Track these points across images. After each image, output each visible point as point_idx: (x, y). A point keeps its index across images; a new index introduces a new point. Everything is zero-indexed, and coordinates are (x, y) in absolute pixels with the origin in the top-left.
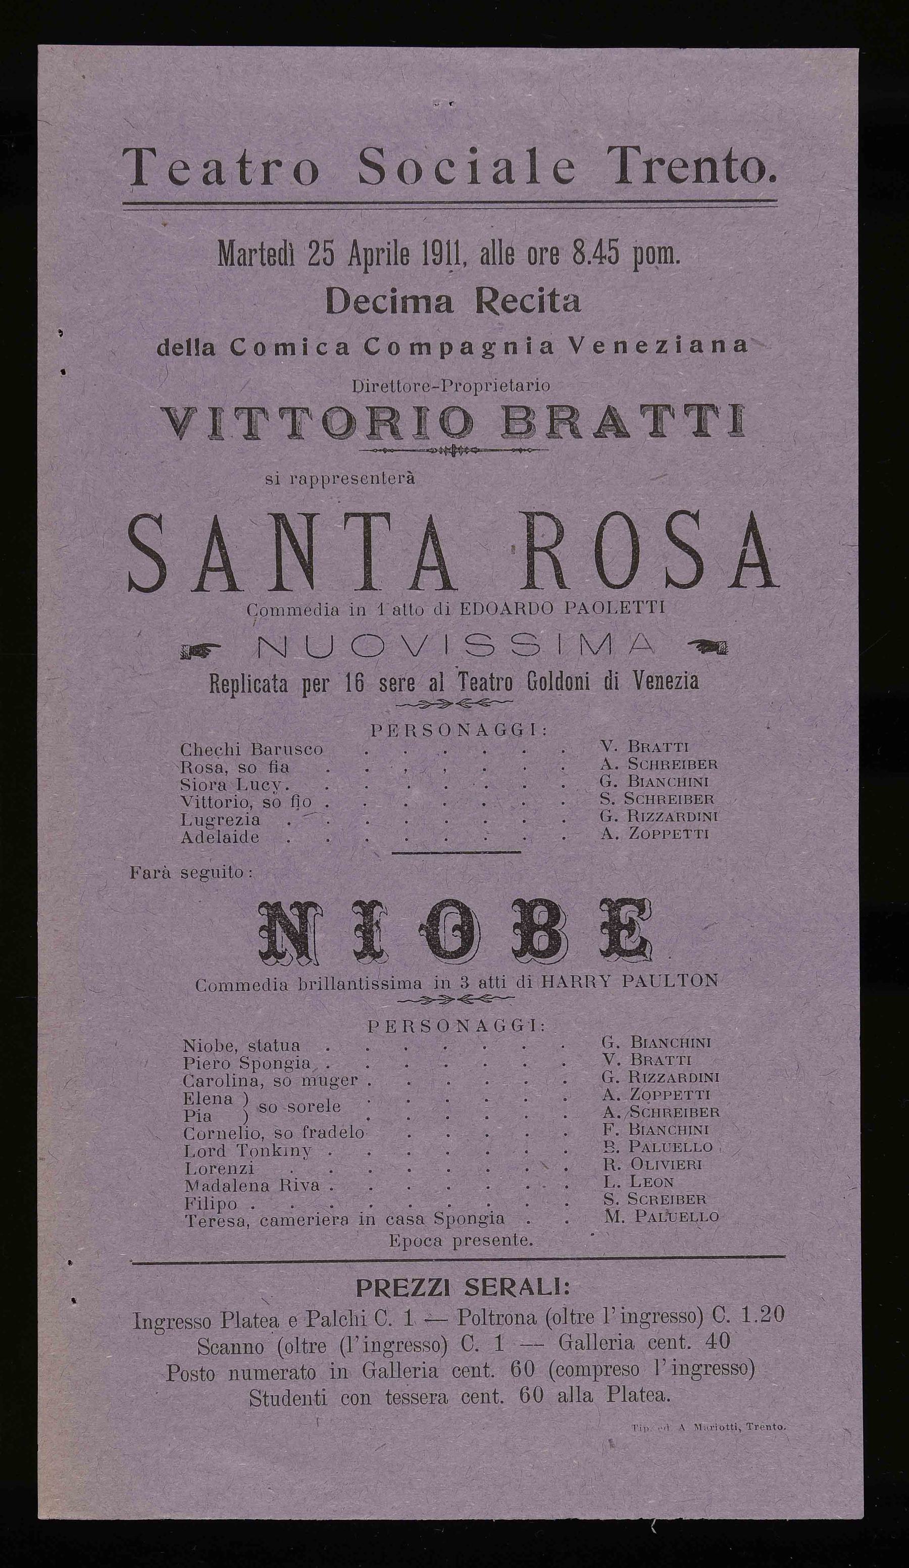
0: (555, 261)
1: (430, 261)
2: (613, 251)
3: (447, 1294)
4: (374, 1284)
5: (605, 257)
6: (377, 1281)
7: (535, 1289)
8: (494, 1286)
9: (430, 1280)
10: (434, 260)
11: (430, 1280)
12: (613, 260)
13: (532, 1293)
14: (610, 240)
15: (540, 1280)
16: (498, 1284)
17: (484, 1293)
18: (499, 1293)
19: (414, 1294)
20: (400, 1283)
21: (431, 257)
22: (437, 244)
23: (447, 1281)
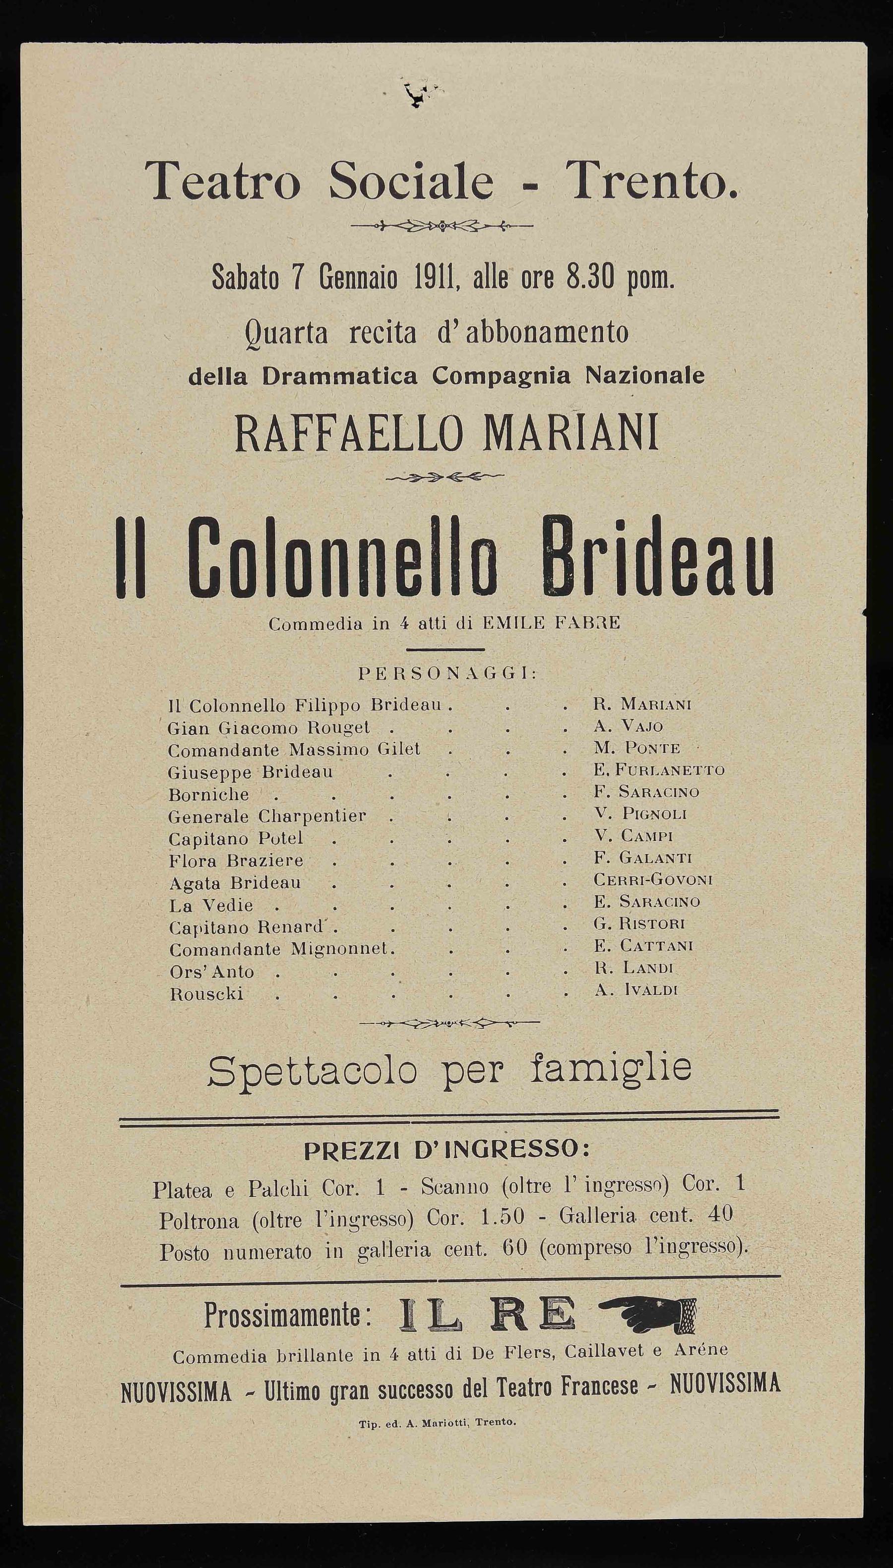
3: (397, 1157)
9: (379, 1143)
11: (379, 1143)
19: (363, 1157)
20: (348, 1147)
23: (396, 1144)
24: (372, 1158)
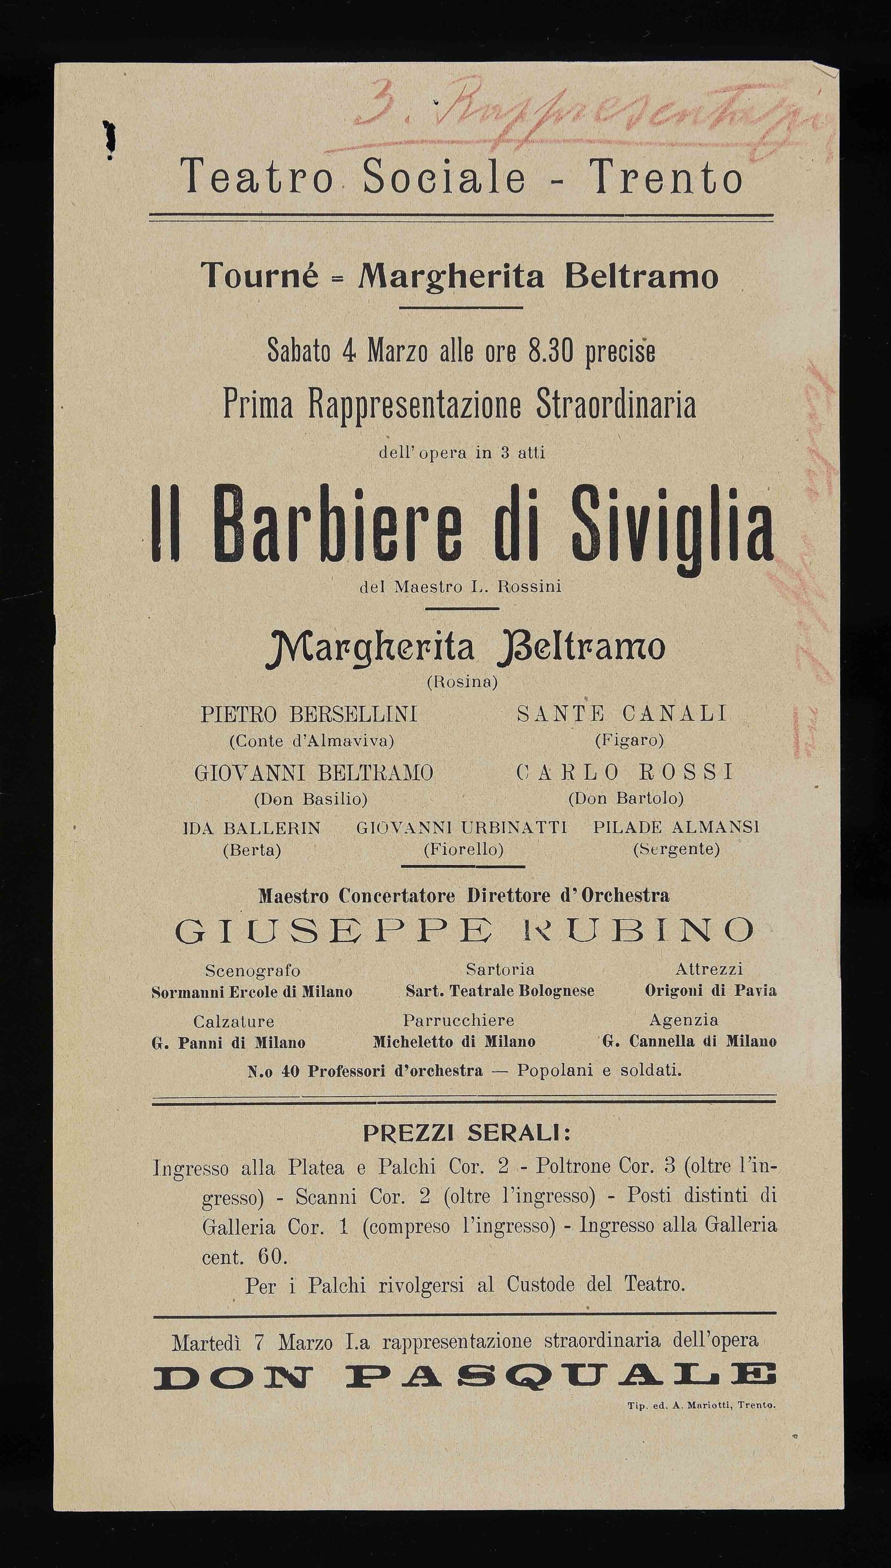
3: (451, 1139)
6: (383, 1127)
7: (535, 1133)
8: (496, 1132)
9: (434, 1126)
11: (434, 1126)
13: (532, 1139)
15: (539, 1126)
16: (500, 1129)
17: (487, 1139)
18: (501, 1138)
19: (419, 1139)
20: (405, 1129)
23: (451, 1126)
24: (427, 1139)
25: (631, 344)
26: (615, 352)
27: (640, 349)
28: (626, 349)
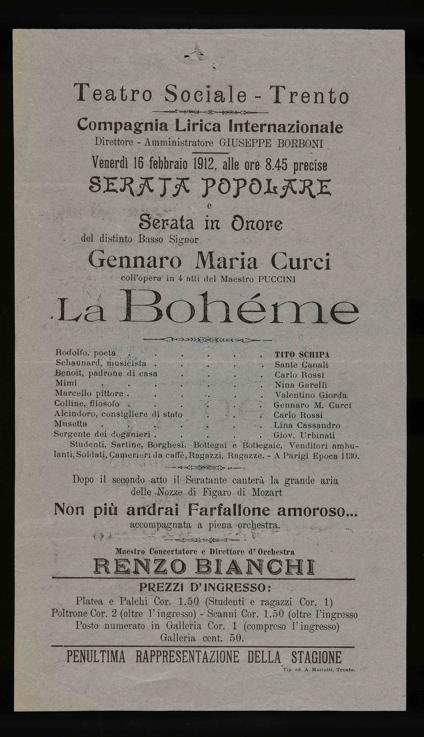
0: (257, 168)
1: (197, 167)
2: (285, 164)
3: (182, 590)
4: (148, 585)
5: (280, 167)
6: (149, 584)
10: (199, 167)
12: (284, 168)
14: (283, 159)
19: (166, 590)
20: (160, 585)
21: (197, 165)
22: (200, 160)
23: (182, 584)
24: (171, 590)
25: (315, 162)
26: (308, 166)
27: (320, 164)
28: (313, 164)
